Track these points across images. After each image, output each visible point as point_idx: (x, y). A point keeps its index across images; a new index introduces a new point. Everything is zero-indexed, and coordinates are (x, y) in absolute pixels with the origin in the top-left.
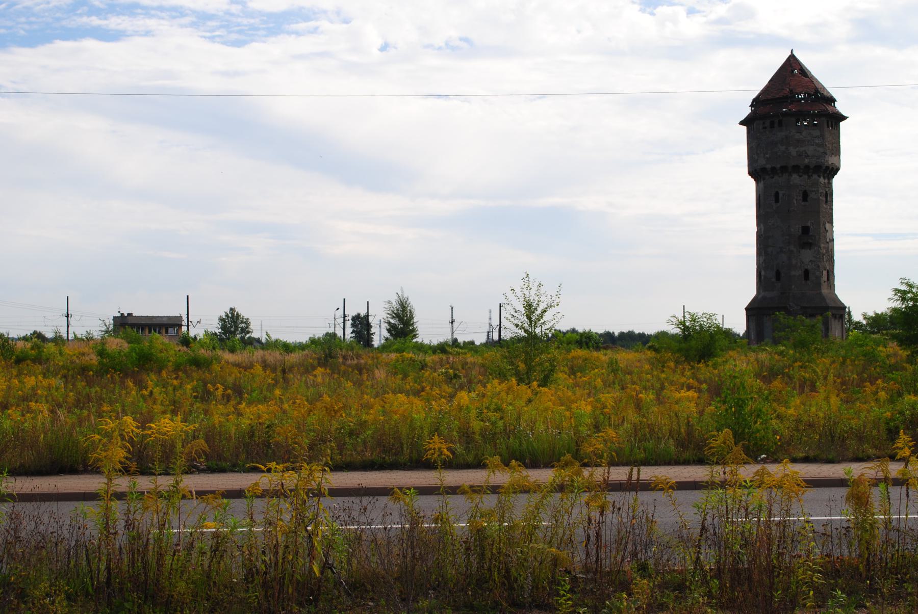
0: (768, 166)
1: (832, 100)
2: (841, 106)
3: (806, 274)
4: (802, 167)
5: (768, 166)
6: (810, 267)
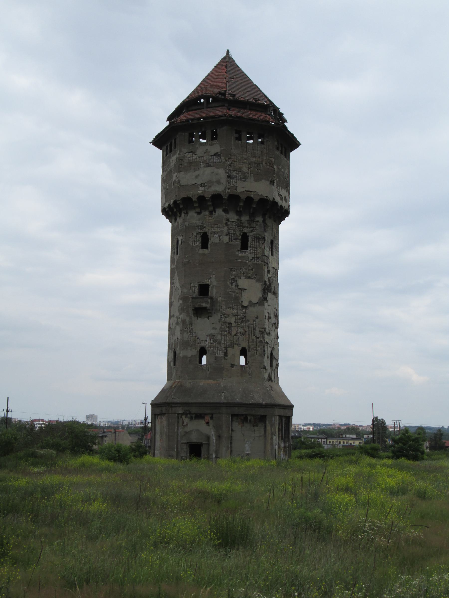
4: (194, 199)
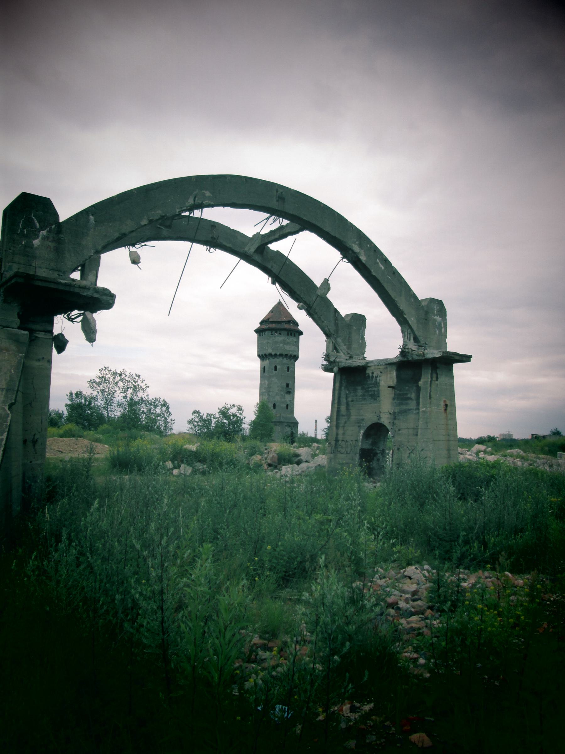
0: (273, 353)
1: (297, 325)
2: (300, 328)
3: (287, 405)
5: (273, 353)
6: (289, 403)
